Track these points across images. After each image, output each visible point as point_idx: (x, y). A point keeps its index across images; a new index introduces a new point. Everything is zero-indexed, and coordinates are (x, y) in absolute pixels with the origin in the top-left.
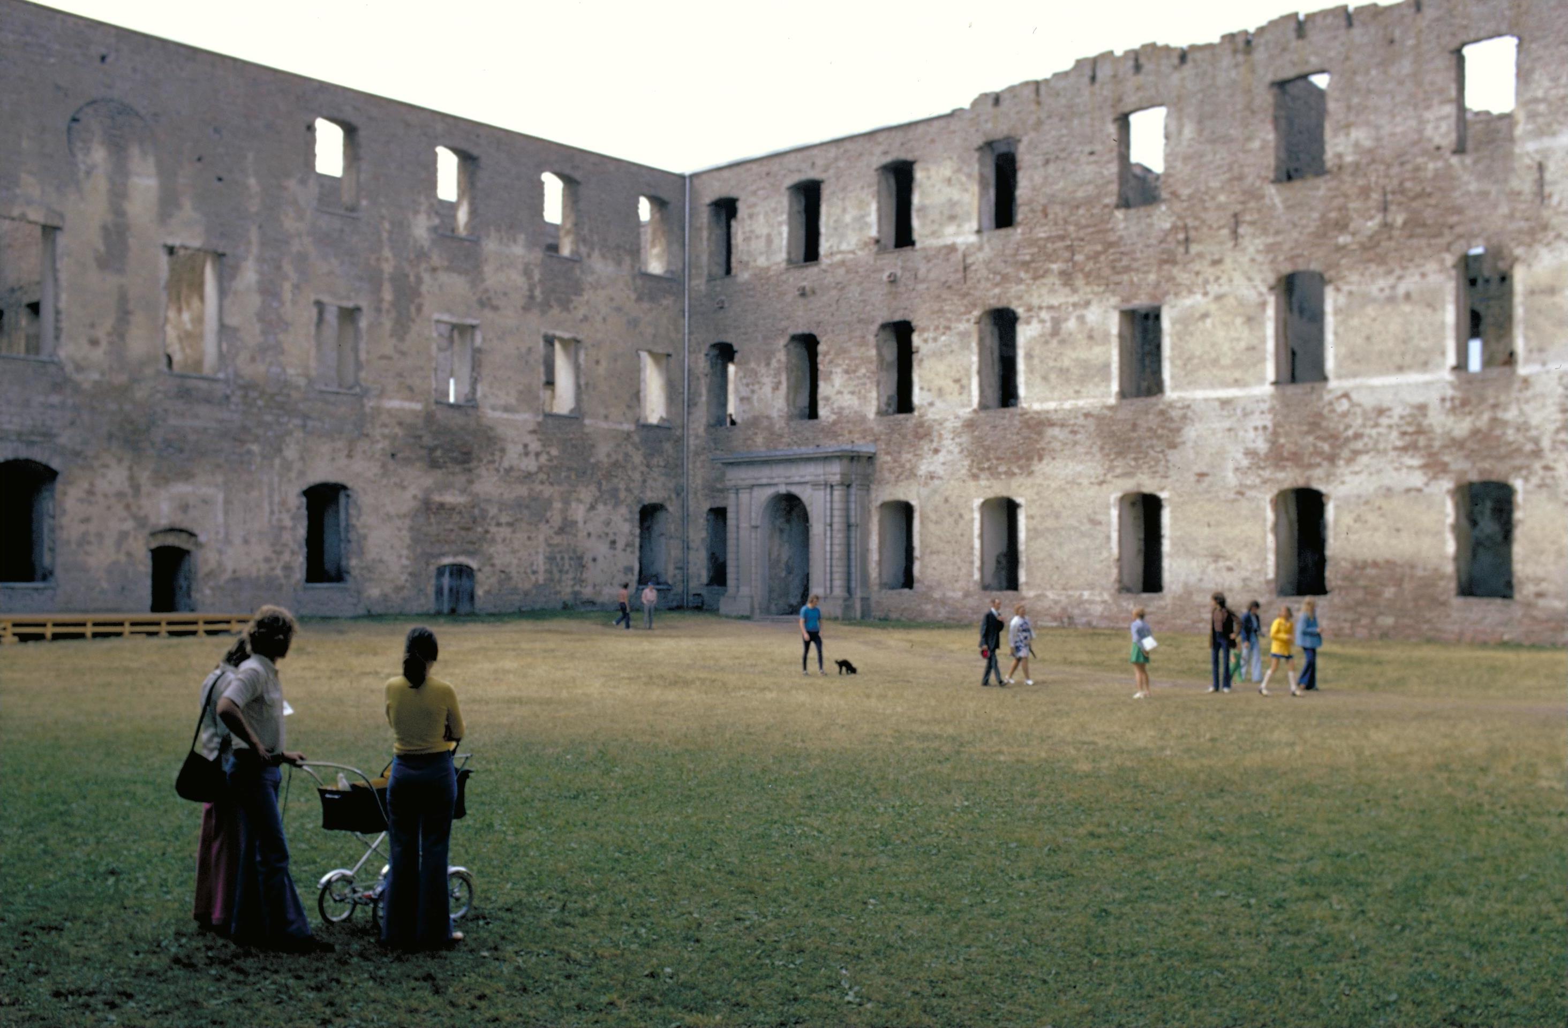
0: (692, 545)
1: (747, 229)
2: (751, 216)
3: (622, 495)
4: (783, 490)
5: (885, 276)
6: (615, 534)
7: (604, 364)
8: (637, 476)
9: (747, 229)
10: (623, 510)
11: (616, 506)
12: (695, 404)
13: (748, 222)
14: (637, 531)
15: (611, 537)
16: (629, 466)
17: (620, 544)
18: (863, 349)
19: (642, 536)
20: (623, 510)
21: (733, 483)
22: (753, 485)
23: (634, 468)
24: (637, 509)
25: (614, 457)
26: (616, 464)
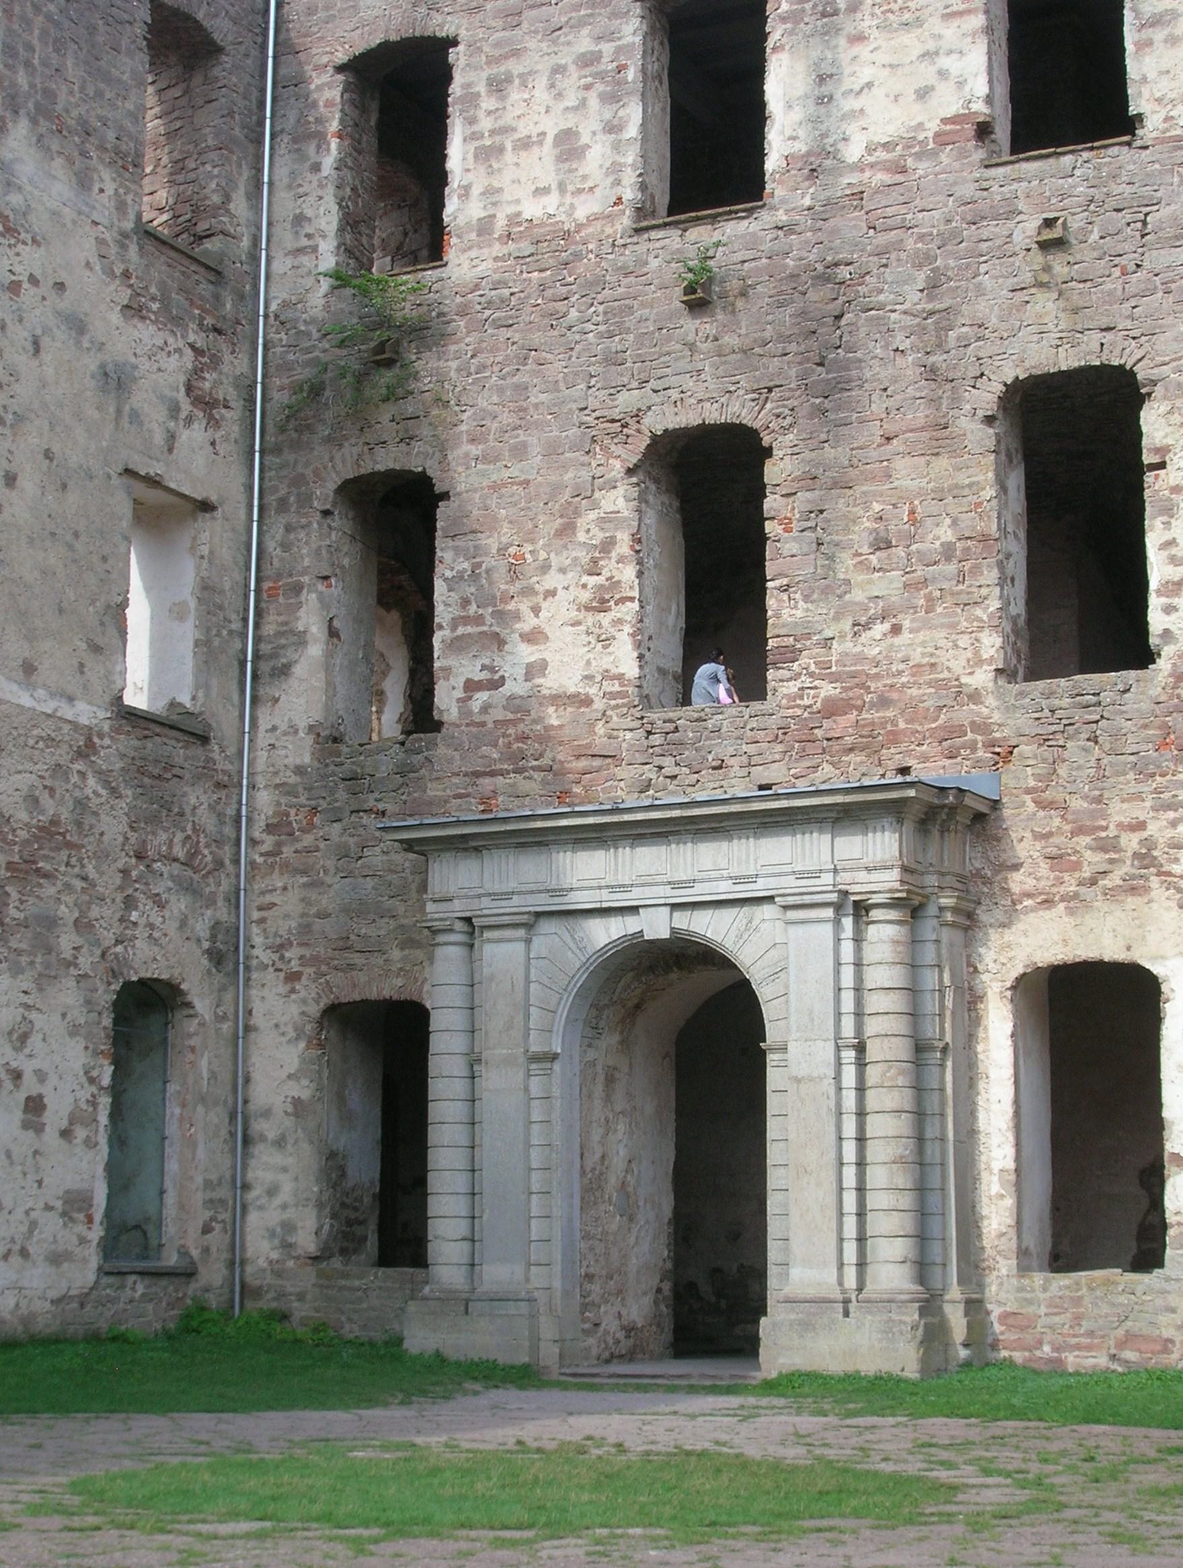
0: (259, 1126)
1: (486, 124)
2: (498, 86)
3: (67, 941)
4: (656, 926)
5: (1027, 229)
6: (41, 1076)
7: (28, 484)
8: (108, 882)
9: (486, 124)
10: (68, 995)
11: (44, 980)
12: (284, 671)
13: (488, 103)
14: (106, 1074)
15: (30, 1086)
16: (90, 843)
17: (56, 1114)
18: (943, 463)
19: (117, 1091)
20: (68, 995)
21: (459, 907)
22: (538, 915)
23: (102, 856)
24: (106, 996)
25: (49, 806)
26: (49, 832)
